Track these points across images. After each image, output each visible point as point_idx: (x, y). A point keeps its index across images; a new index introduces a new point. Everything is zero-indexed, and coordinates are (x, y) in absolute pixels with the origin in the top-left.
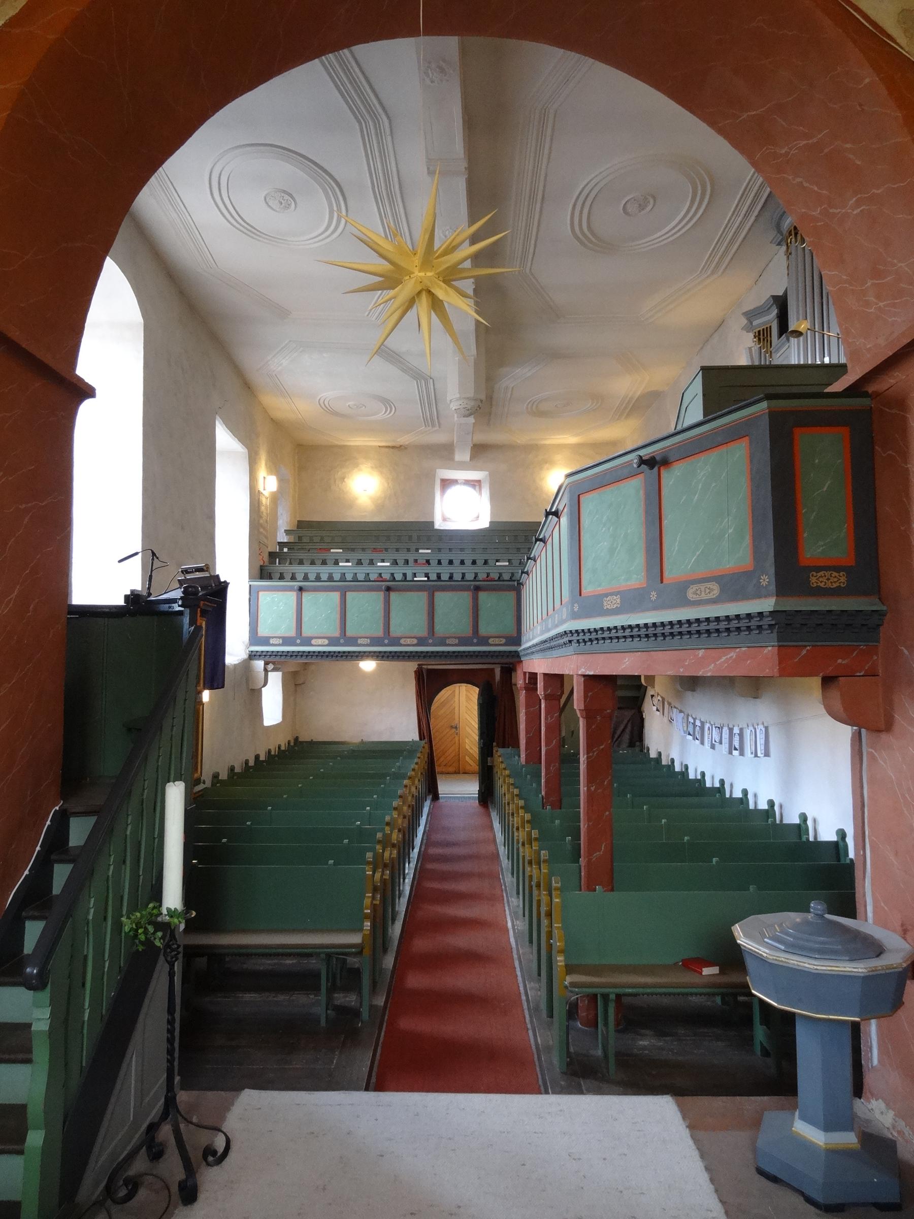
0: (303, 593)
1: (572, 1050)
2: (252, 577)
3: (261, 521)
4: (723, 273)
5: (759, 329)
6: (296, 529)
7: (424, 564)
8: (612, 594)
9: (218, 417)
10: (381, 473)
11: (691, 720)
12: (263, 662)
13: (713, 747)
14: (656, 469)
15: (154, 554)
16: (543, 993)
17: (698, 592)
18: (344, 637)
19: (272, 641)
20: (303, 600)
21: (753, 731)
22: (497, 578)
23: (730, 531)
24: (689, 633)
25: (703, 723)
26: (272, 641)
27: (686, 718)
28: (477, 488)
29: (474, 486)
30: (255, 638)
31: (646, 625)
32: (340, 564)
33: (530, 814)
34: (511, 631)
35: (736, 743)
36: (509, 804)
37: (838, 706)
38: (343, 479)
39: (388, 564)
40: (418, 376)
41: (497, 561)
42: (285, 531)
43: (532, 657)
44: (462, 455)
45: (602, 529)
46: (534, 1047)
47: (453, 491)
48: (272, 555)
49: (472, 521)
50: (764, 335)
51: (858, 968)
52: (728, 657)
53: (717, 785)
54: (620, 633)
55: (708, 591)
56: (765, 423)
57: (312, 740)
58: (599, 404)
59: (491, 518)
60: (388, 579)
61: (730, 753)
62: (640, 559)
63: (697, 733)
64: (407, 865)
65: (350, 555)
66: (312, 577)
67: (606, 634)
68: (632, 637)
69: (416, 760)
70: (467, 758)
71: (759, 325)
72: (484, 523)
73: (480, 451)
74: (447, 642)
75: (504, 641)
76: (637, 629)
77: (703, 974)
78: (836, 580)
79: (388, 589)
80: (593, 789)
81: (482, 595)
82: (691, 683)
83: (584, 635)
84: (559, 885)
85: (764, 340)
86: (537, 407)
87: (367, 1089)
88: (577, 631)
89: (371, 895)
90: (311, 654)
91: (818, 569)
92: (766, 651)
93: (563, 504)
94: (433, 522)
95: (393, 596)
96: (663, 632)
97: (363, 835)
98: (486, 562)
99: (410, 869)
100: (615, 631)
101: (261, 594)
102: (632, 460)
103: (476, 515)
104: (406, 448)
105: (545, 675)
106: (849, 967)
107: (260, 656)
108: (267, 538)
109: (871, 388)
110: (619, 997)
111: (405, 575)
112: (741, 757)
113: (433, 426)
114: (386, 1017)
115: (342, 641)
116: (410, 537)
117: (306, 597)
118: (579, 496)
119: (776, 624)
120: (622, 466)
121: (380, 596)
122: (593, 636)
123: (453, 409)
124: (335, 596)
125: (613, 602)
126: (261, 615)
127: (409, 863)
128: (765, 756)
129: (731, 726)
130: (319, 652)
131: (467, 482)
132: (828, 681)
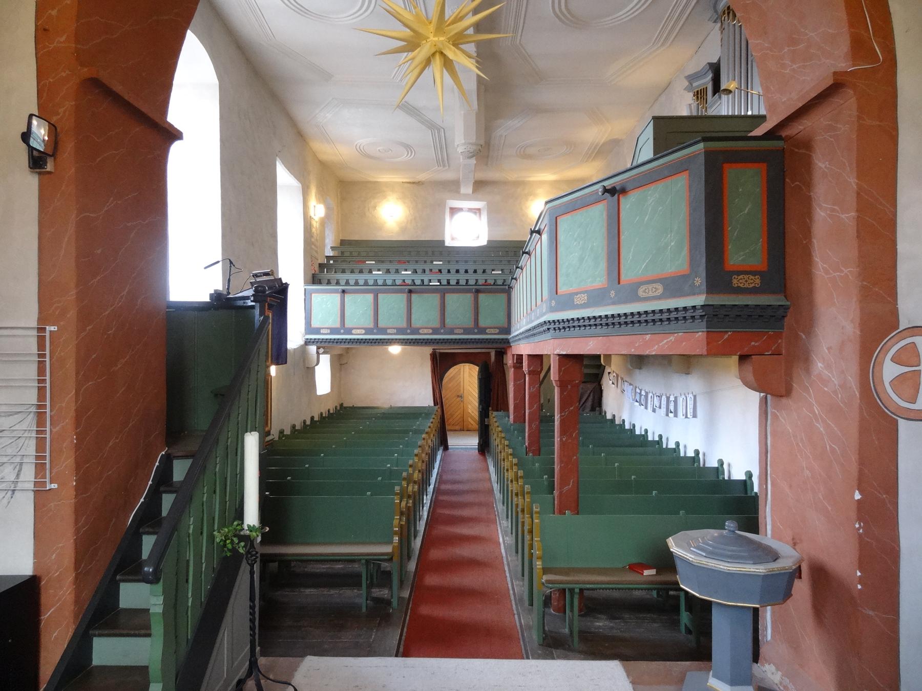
0: (346, 295)
1: (546, 628)
2: (306, 283)
3: (313, 240)
4: (670, 45)
5: (697, 90)
7: (437, 273)
8: (580, 293)
9: (278, 159)
10: (404, 203)
11: (638, 391)
12: (315, 347)
13: (654, 411)
14: (616, 195)
15: (231, 263)
16: (526, 589)
17: (647, 291)
19: (322, 331)
20: (346, 300)
21: (685, 399)
22: (492, 284)
23: (672, 244)
24: (639, 322)
25: (647, 393)
27: (634, 389)
28: (478, 214)
29: (475, 213)
30: (309, 328)
31: (606, 316)
32: (374, 273)
33: (517, 459)
34: (503, 322)
35: (672, 408)
36: (501, 452)
37: (750, 377)
38: (375, 207)
39: (410, 273)
40: (432, 126)
41: (493, 270)
42: (331, 247)
43: (519, 342)
44: (467, 189)
45: (574, 243)
46: (519, 627)
47: (458, 216)
48: (321, 266)
49: (474, 240)
50: (701, 94)
51: (760, 569)
52: (669, 340)
53: (657, 439)
54: (587, 323)
55: (654, 290)
56: (702, 159)
58: (572, 148)
59: (488, 238)
60: (410, 284)
61: (667, 415)
62: (603, 265)
63: (643, 401)
64: (425, 497)
65: (381, 266)
66: (352, 282)
67: (576, 324)
68: (596, 325)
69: (431, 420)
71: (697, 87)
72: (483, 242)
73: (480, 185)
75: (497, 331)
76: (600, 320)
77: (644, 574)
78: (752, 281)
79: (410, 291)
80: (564, 439)
81: (482, 296)
82: (639, 361)
83: (559, 324)
84: (538, 510)
85: (701, 98)
86: (524, 152)
87: (396, 656)
88: (554, 321)
89: (398, 517)
90: (352, 341)
91: (739, 273)
92: (698, 335)
93: (544, 225)
94: (444, 241)
95: (414, 296)
96: (619, 321)
97: (392, 474)
98: (484, 271)
99: (427, 500)
100: (583, 321)
101: (313, 295)
102: (598, 190)
105: (529, 356)
106: (753, 569)
107: (313, 342)
108: (316, 252)
109: (784, 133)
110: (581, 590)
111: (422, 281)
112: (675, 418)
113: (444, 166)
114: (410, 606)
116: (427, 253)
117: (348, 297)
118: (556, 218)
119: (705, 315)
120: (591, 194)
122: (566, 325)
123: (460, 152)
124: (370, 297)
125: (581, 299)
127: (427, 495)
128: (693, 417)
129: (668, 395)
130: (358, 339)
131: (470, 210)
132: (743, 358)
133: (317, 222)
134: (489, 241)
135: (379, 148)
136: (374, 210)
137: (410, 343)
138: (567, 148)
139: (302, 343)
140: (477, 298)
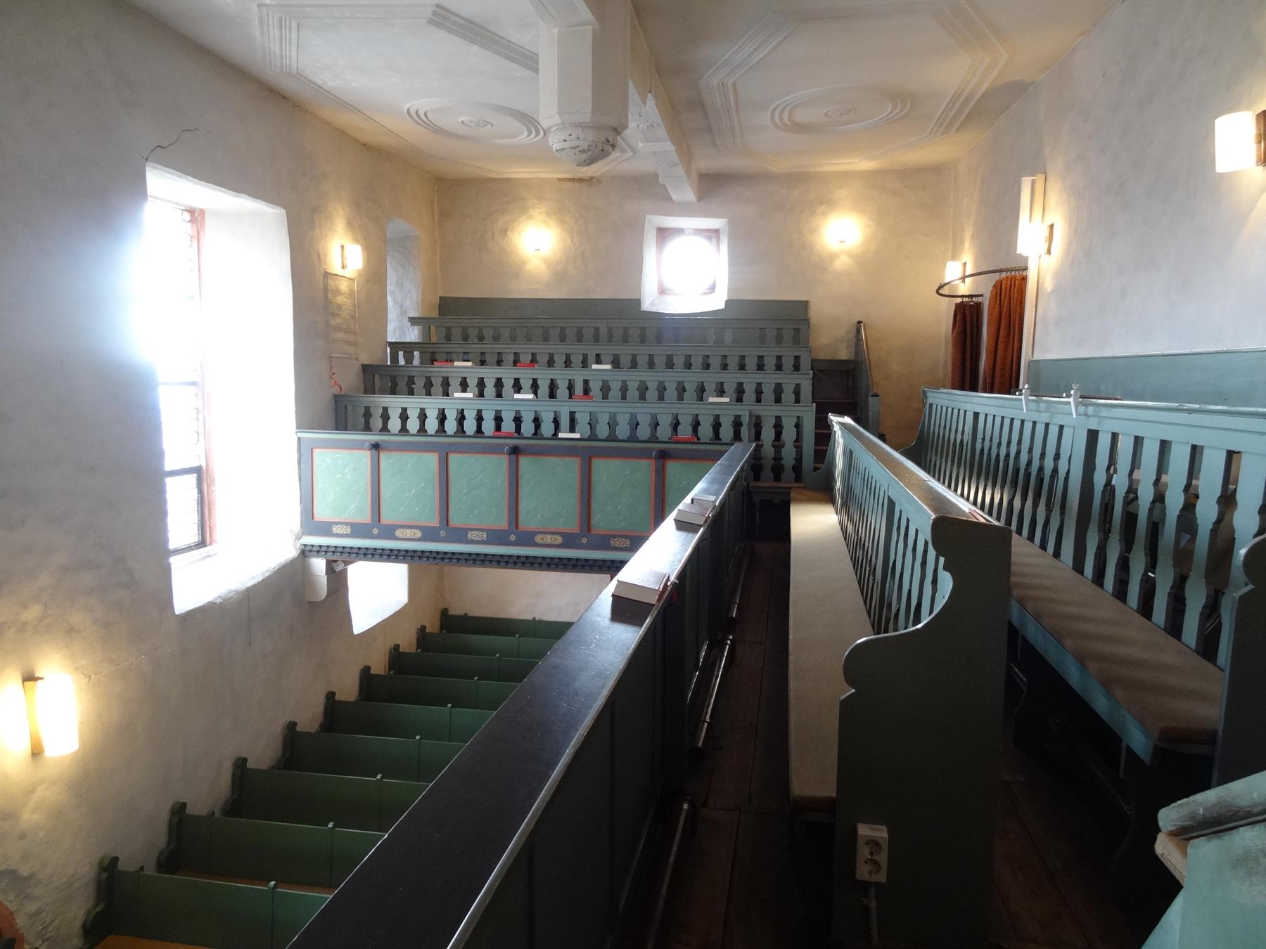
0: (380, 452)
2: (302, 424)
10: (562, 222)
12: (324, 561)
20: (382, 465)
26: (335, 529)
28: (714, 240)
29: (710, 238)
38: (504, 232)
47: (675, 245)
49: (705, 294)
57: (466, 614)
58: (907, 109)
59: (730, 290)
72: (717, 302)
94: (640, 300)
95: (524, 461)
101: (317, 452)
103: (708, 284)
104: (599, 181)
117: (386, 459)
121: (503, 461)
131: (699, 232)
134: (727, 302)
135: (461, 120)
136: (504, 238)
137: (515, 563)
138: (895, 107)
139: (291, 553)
140: (664, 470)
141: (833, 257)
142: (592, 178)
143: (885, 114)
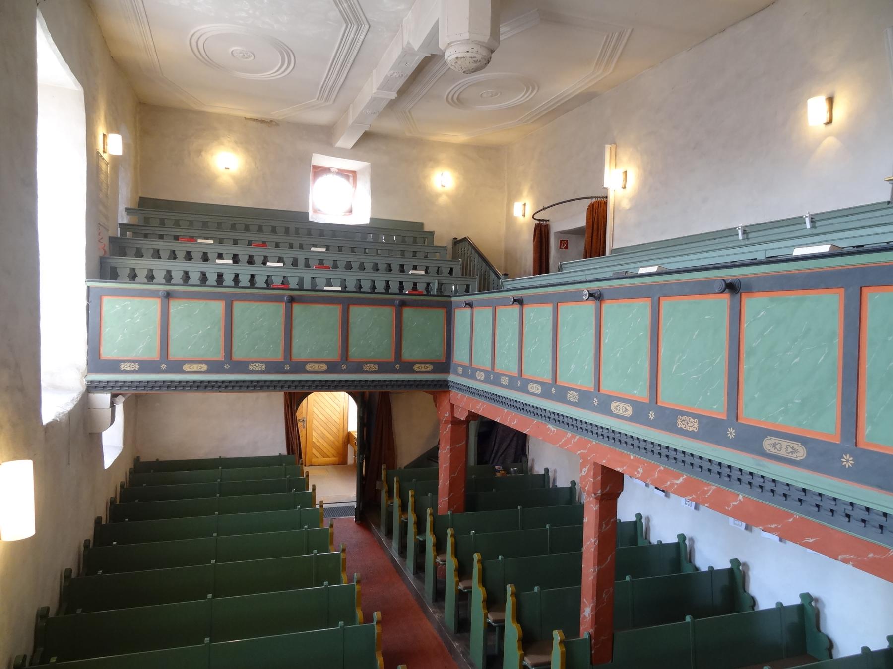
2: (90, 276)
3: (101, 196)
6: (137, 208)
12: (109, 395)
18: (230, 362)
20: (172, 311)
28: (351, 179)
29: (347, 177)
30: (95, 361)
34: (440, 355)
38: (199, 152)
42: (127, 209)
44: (346, 141)
47: (324, 181)
48: (112, 240)
57: (157, 460)
59: (371, 215)
70: (314, 451)
74: (365, 368)
75: (430, 367)
79: (292, 300)
81: (407, 312)
90: (183, 384)
94: (308, 213)
95: (297, 308)
101: (106, 300)
103: (348, 208)
115: (227, 366)
117: (177, 307)
121: (280, 308)
124: (218, 307)
126: (106, 331)
131: (341, 173)
133: (107, 164)
134: (371, 219)
141: (438, 195)
142: (271, 121)
143: (518, 98)
